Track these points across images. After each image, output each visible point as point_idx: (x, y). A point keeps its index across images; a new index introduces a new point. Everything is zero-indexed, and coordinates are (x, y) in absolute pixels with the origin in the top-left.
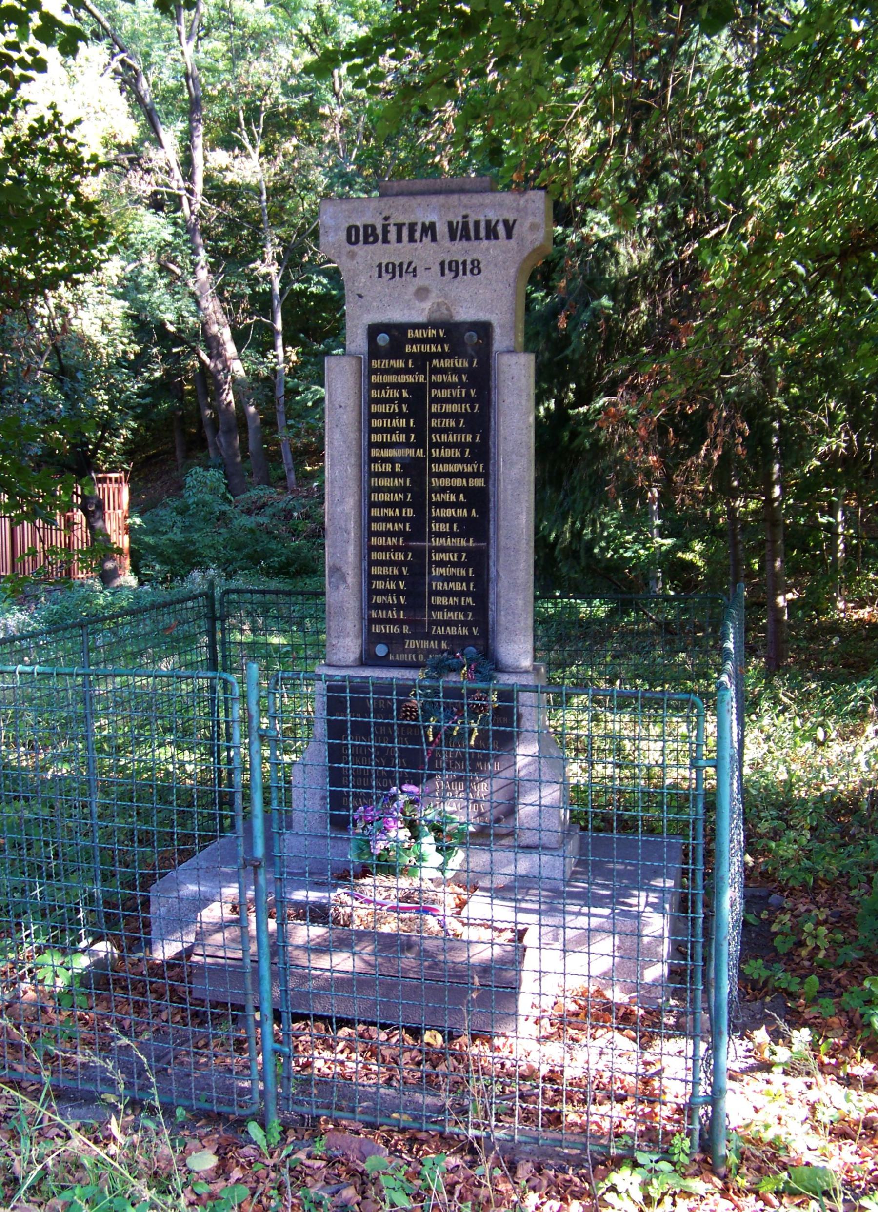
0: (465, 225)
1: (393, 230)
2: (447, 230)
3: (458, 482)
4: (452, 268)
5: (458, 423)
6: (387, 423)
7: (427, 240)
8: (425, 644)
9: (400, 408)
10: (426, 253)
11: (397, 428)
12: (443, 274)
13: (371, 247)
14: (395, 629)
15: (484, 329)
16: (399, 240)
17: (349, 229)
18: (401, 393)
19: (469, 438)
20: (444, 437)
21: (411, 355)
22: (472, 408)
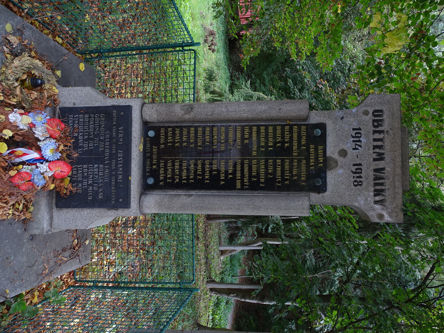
0: (382, 178)
1: (381, 136)
2: (380, 167)
3: (239, 174)
4: (358, 170)
5: (270, 174)
6: (271, 135)
7: (375, 156)
8: (155, 157)
9: (279, 142)
10: (366, 155)
11: (268, 140)
12: (354, 165)
13: (371, 124)
14: (162, 141)
15: (322, 189)
16: (375, 140)
17: (381, 111)
18: (287, 142)
19: (262, 180)
20: (263, 167)
21: (308, 149)
22: (279, 182)
